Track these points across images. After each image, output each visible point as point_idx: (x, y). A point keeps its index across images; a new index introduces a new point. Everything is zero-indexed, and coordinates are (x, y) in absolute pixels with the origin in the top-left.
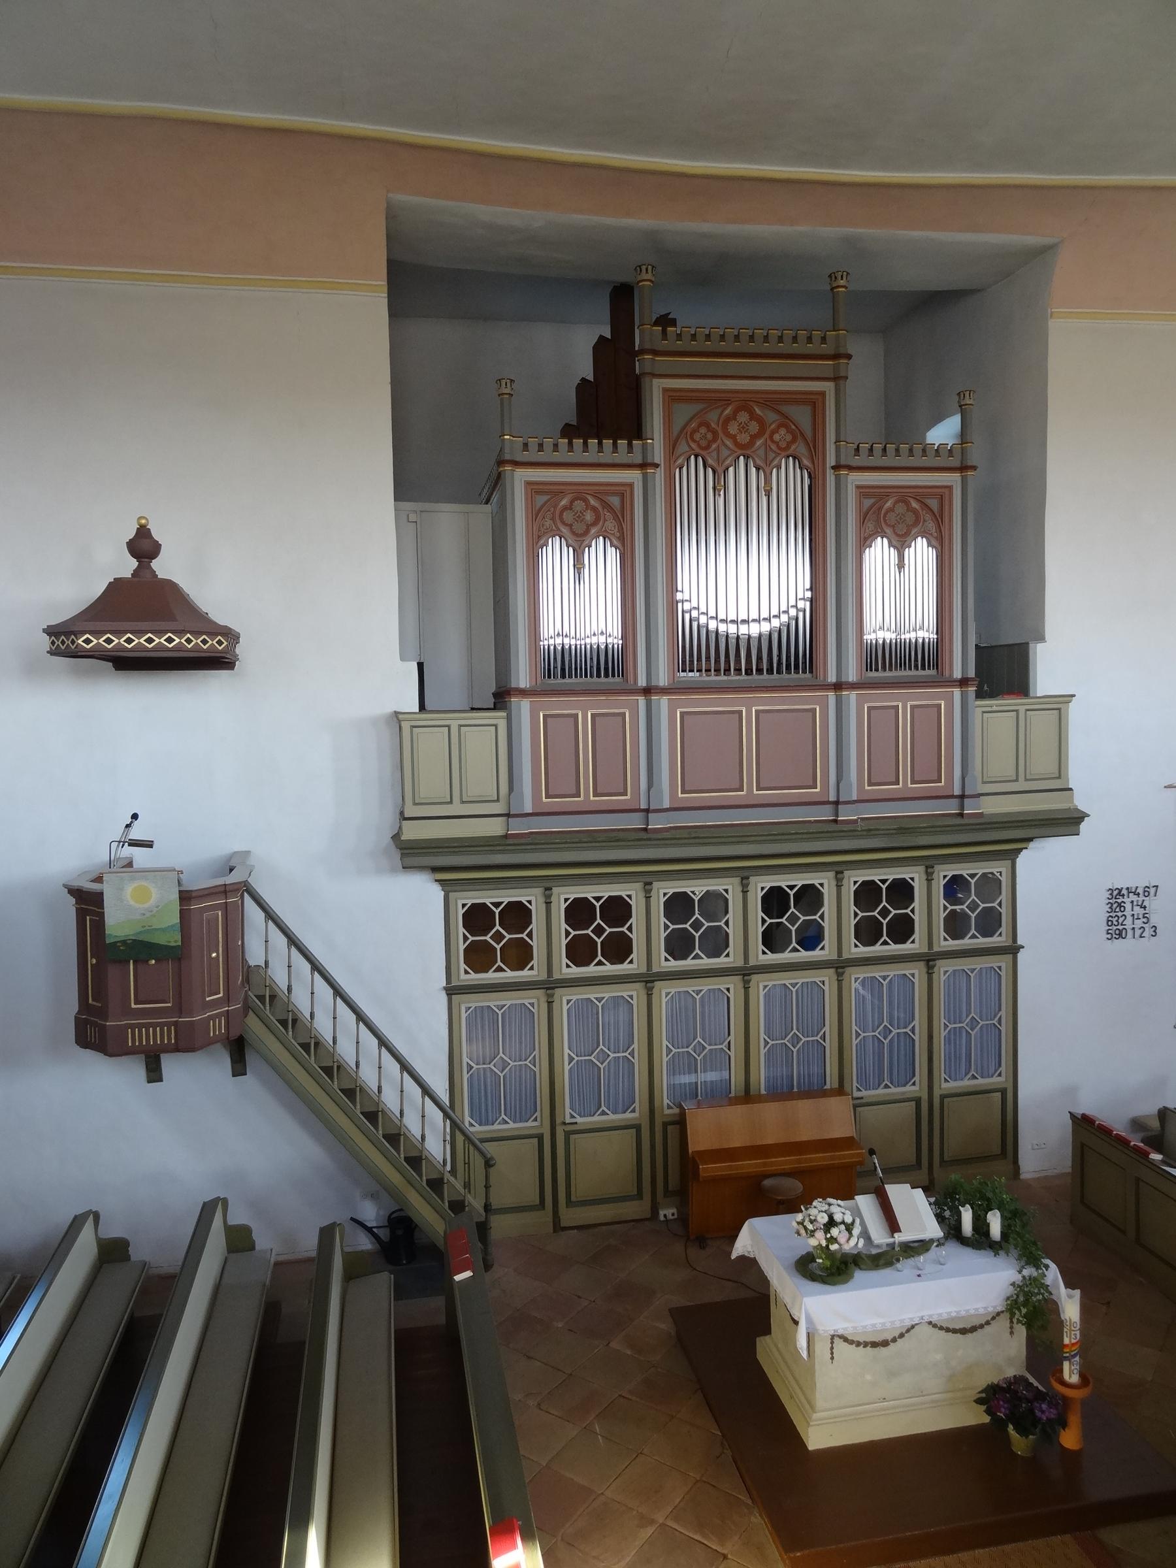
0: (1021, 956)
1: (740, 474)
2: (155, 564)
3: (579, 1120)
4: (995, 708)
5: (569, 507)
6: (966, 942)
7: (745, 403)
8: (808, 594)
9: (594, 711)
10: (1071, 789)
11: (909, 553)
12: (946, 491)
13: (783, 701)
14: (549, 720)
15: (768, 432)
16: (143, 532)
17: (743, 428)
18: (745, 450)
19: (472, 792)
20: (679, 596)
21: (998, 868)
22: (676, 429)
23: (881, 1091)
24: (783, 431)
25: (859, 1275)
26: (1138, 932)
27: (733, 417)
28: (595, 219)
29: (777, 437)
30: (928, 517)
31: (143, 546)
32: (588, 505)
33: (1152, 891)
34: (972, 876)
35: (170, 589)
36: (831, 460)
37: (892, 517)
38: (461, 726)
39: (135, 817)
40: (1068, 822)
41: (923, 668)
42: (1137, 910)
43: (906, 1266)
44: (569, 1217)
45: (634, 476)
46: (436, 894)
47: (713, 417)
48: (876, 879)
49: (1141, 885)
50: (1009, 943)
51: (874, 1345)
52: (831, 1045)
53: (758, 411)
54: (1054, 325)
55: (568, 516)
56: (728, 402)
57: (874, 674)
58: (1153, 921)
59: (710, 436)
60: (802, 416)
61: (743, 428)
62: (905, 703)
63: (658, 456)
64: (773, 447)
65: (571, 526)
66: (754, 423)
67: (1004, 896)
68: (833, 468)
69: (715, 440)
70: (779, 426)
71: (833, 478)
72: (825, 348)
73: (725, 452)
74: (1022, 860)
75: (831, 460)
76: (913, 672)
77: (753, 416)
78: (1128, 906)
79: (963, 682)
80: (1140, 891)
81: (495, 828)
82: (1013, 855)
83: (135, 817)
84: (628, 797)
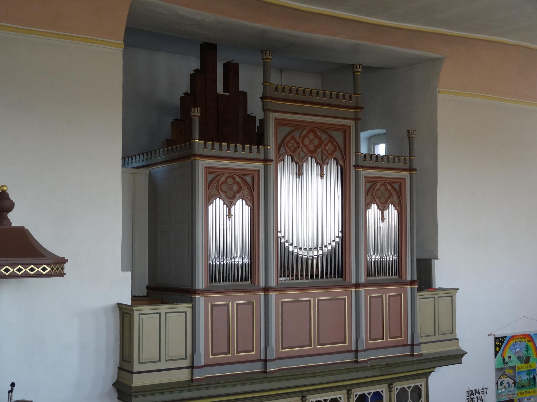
4: (426, 296)
5: (225, 182)
7: (313, 128)
8: (340, 234)
9: (238, 302)
10: (457, 339)
11: (386, 212)
12: (403, 181)
13: (330, 294)
14: (214, 308)
15: (324, 144)
17: (311, 142)
18: (312, 153)
19: (172, 354)
20: (279, 234)
22: (279, 141)
24: (330, 145)
27: (307, 136)
29: (327, 148)
30: (394, 194)
32: (235, 182)
33: (485, 390)
34: (409, 388)
35: (22, 232)
38: (166, 313)
39: (13, 385)
40: (456, 357)
41: (392, 275)
45: (260, 166)
47: (297, 134)
49: (479, 387)
53: (319, 134)
54: (439, 95)
55: (224, 187)
57: (373, 278)
59: (295, 145)
60: (338, 137)
64: (326, 153)
65: (225, 192)
66: (316, 139)
68: (354, 166)
69: (298, 147)
71: (354, 171)
72: (352, 103)
73: (302, 155)
74: (431, 378)
76: (388, 277)
77: (316, 136)
79: (412, 283)
80: (480, 391)
81: (184, 376)
82: (426, 376)
83: (13, 385)
84: (254, 353)
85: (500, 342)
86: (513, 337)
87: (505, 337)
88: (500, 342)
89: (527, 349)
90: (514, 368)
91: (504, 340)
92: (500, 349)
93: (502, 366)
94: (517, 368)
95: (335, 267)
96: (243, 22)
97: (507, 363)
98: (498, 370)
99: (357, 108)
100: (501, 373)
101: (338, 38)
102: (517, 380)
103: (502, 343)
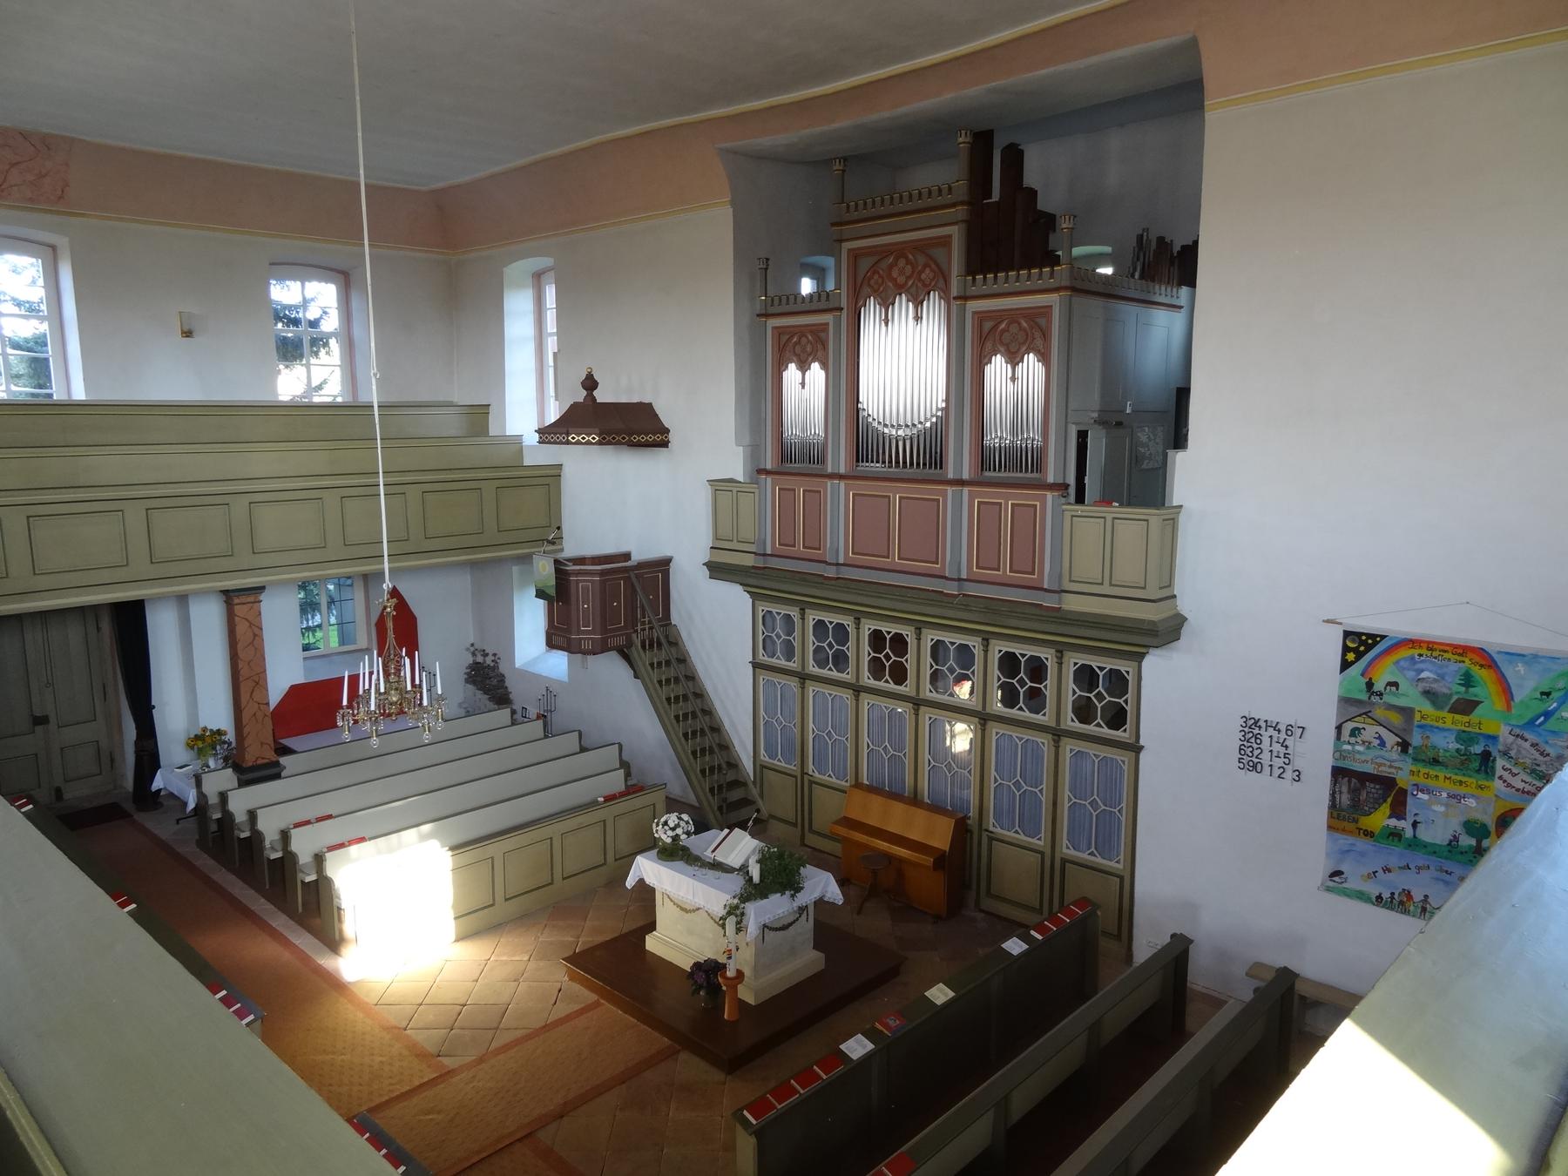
1: (903, 308)
2: (595, 393)
3: (816, 774)
5: (798, 343)
6: (1090, 729)
7: (899, 251)
17: (902, 272)
18: (900, 289)
21: (1123, 666)
23: (1011, 834)
25: (680, 864)
26: (1277, 772)
28: (818, 129)
31: (590, 384)
36: (954, 292)
42: (1277, 747)
43: (711, 873)
44: (811, 839)
45: (827, 318)
48: (1017, 652)
50: (1132, 741)
51: (683, 909)
55: (798, 349)
58: (1298, 763)
60: (939, 253)
62: (1008, 500)
63: (844, 304)
70: (926, 266)
74: (1147, 663)
77: (908, 262)
78: (1266, 740)
80: (1282, 728)
81: (749, 561)
82: (1143, 655)
85: (1359, 645)
87: (1383, 637)
88: (1359, 645)
89: (1468, 681)
90: (1407, 712)
91: (1375, 644)
92: (1358, 659)
93: (1364, 696)
94: (1417, 716)
95: (926, 454)
96: (825, 128)
97: (1380, 695)
98: (1345, 701)
99: (953, 205)
102: (1416, 739)
103: (1369, 648)
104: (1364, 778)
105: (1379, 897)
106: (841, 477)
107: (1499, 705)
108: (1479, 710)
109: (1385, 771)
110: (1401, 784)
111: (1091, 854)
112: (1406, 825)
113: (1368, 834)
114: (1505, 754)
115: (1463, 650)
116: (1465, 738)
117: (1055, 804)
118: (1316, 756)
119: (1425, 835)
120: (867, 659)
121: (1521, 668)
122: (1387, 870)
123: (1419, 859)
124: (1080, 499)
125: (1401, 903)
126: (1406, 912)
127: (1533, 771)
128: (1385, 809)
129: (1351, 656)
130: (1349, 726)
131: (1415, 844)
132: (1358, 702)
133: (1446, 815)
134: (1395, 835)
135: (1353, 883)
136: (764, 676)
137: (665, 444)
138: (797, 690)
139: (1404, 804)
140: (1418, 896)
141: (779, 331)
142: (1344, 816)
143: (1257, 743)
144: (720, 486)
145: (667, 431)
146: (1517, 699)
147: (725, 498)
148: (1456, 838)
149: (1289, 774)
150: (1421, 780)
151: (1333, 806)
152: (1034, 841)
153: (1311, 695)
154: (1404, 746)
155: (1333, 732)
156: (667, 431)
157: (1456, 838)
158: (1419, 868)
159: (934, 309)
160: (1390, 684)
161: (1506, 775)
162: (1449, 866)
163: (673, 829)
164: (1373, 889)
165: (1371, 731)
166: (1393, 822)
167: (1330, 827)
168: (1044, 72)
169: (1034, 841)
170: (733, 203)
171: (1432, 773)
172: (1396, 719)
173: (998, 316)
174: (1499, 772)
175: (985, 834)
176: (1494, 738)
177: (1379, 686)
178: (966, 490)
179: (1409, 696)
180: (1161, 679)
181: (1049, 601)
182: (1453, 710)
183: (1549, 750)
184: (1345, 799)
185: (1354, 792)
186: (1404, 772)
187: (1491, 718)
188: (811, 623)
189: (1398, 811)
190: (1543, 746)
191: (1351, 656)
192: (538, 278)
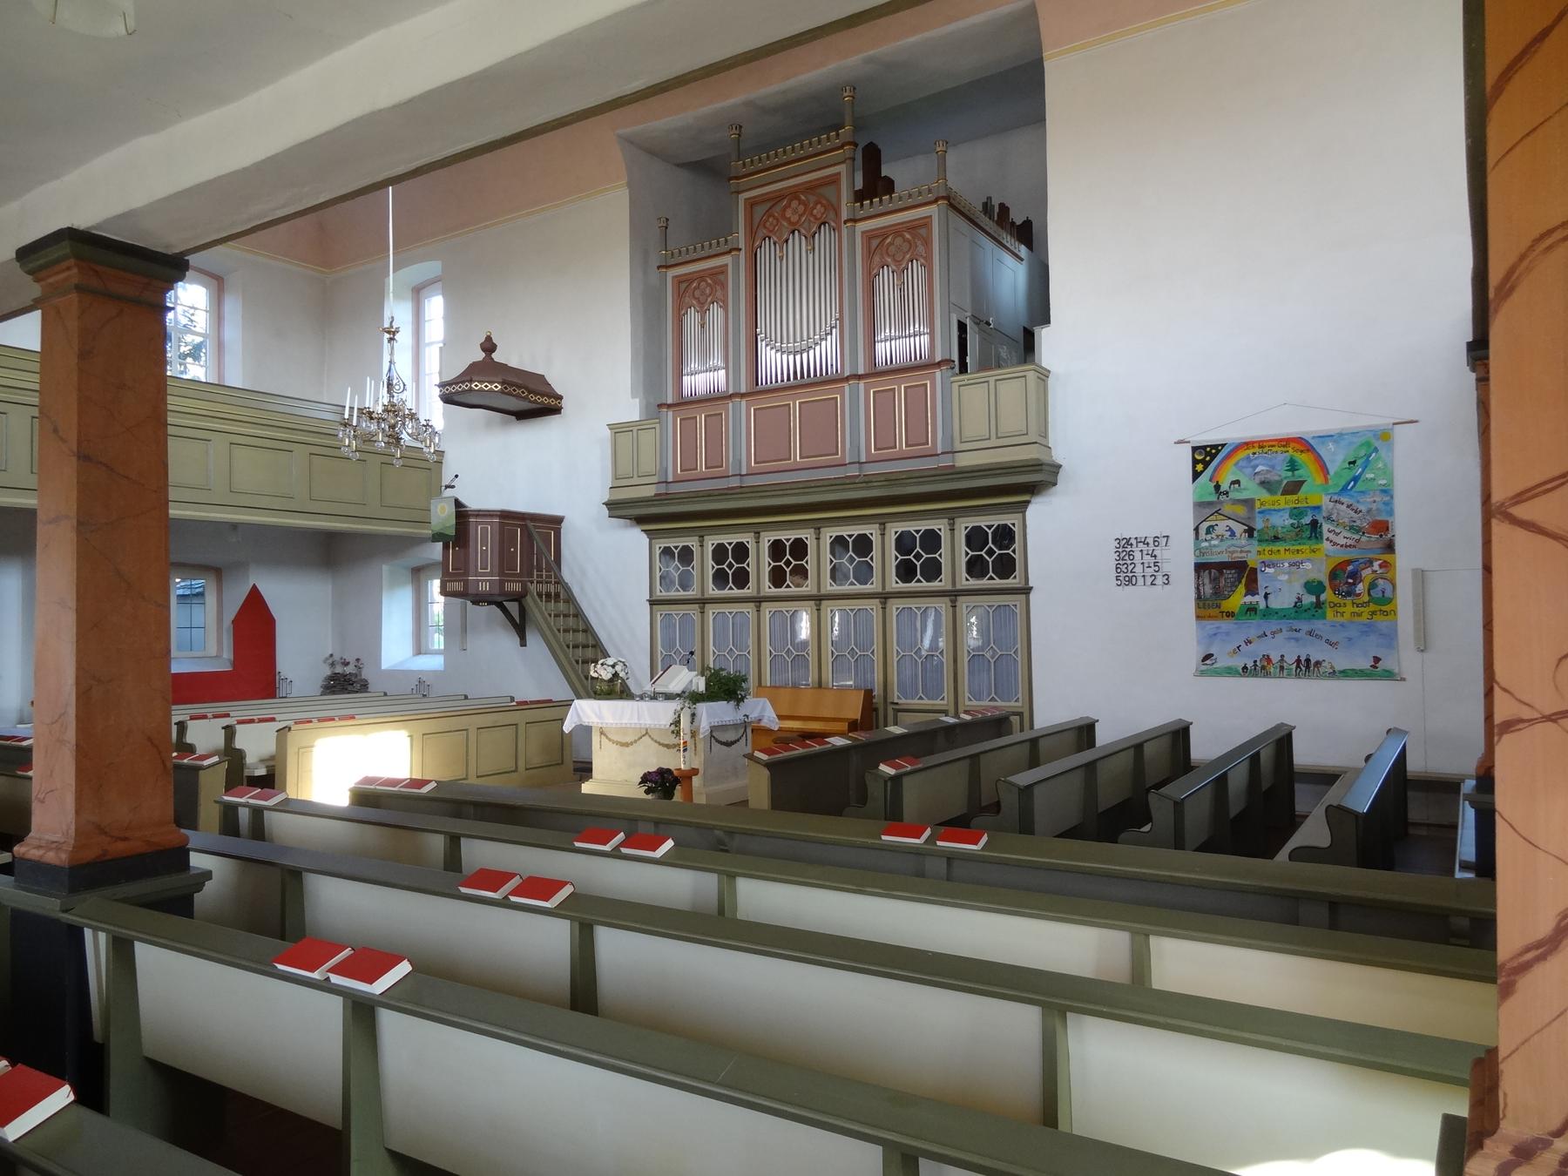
0: (1032, 596)
1: (797, 243)
5: (698, 287)
7: (793, 194)
16: (489, 339)
17: (795, 212)
26: (1149, 580)
27: (788, 206)
31: (489, 347)
36: (844, 216)
37: (892, 249)
42: (1147, 559)
45: (727, 260)
46: (645, 539)
48: (911, 529)
49: (1150, 534)
52: (878, 658)
55: (697, 293)
56: (782, 197)
58: (1166, 568)
61: (795, 212)
67: (1017, 545)
75: (844, 216)
78: (1137, 555)
80: (1150, 541)
81: (650, 492)
85: (1205, 456)
86: (1247, 445)
88: (1205, 456)
89: (1293, 466)
90: (1249, 503)
91: (1218, 452)
93: (1213, 498)
94: (1258, 504)
98: (1199, 505)
99: (842, 147)
100: (1208, 511)
101: (832, 66)
102: (1259, 524)
103: (1213, 457)
104: (1221, 567)
105: (1245, 668)
106: (743, 395)
107: (1319, 480)
108: (1304, 488)
109: (1238, 557)
110: (1251, 564)
111: (993, 699)
112: (1258, 599)
113: (1230, 615)
114: (1328, 518)
115: (1285, 442)
116: (1297, 513)
117: (955, 661)
118: (1180, 559)
119: (1275, 603)
120: (767, 569)
121: (1331, 445)
122: (1248, 642)
123: (1273, 625)
124: (963, 369)
125: (1263, 668)
126: (1267, 675)
127: (1351, 528)
128: (1241, 589)
129: (1200, 467)
130: (1205, 525)
131: (1269, 613)
132: (1210, 504)
133: (1289, 581)
134: (1251, 609)
135: (1222, 662)
136: (661, 611)
137: (556, 410)
138: (696, 617)
139: (1256, 581)
140: (1275, 658)
141: (679, 280)
142: (1208, 606)
143: (1131, 560)
144: (617, 429)
145: (560, 398)
146: (1332, 472)
147: (625, 439)
148: (1299, 599)
149: (1160, 580)
150: (1266, 557)
151: (1199, 597)
152: (938, 702)
153: (1168, 508)
154: (1250, 532)
155: (1192, 533)
156: (560, 398)
157: (1299, 599)
158: (1274, 633)
159: (824, 237)
160: (1233, 483)
161: (1331, 536)
162: (1297, 624)
163: (613, 666)
164: (1238, 663)
165: (1222, 526)
166: (1249, 599)
167: (1198, 617)
168: (911, 39)
169: (938, 702)
170: (630, 185)
171: (1275, 548)
172: (1241, 511)
173: (882, 234)
174: (1326, 534)
175: (890, 708)
176: (1318, 508)
177: (1224, 487)
178: (862, 384)
179: (1250, 489)
180: (1044, 526)
181: (945, 462)
182: (1285, 492)
183: (1361, 507)
184: (1208, 589)
185: (1214, 581)
186: (1252, 553)
187: (1315, 493)
188: (711, 549)
189: (1252, 589)
190: (1356, 505)
191: (1200, 467)
192: (418, 293)
